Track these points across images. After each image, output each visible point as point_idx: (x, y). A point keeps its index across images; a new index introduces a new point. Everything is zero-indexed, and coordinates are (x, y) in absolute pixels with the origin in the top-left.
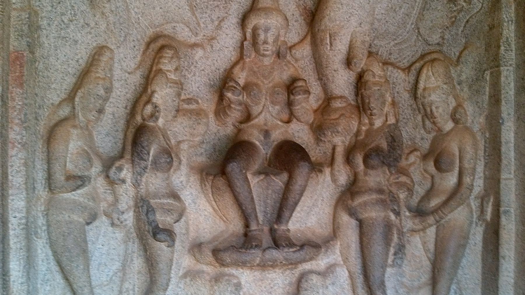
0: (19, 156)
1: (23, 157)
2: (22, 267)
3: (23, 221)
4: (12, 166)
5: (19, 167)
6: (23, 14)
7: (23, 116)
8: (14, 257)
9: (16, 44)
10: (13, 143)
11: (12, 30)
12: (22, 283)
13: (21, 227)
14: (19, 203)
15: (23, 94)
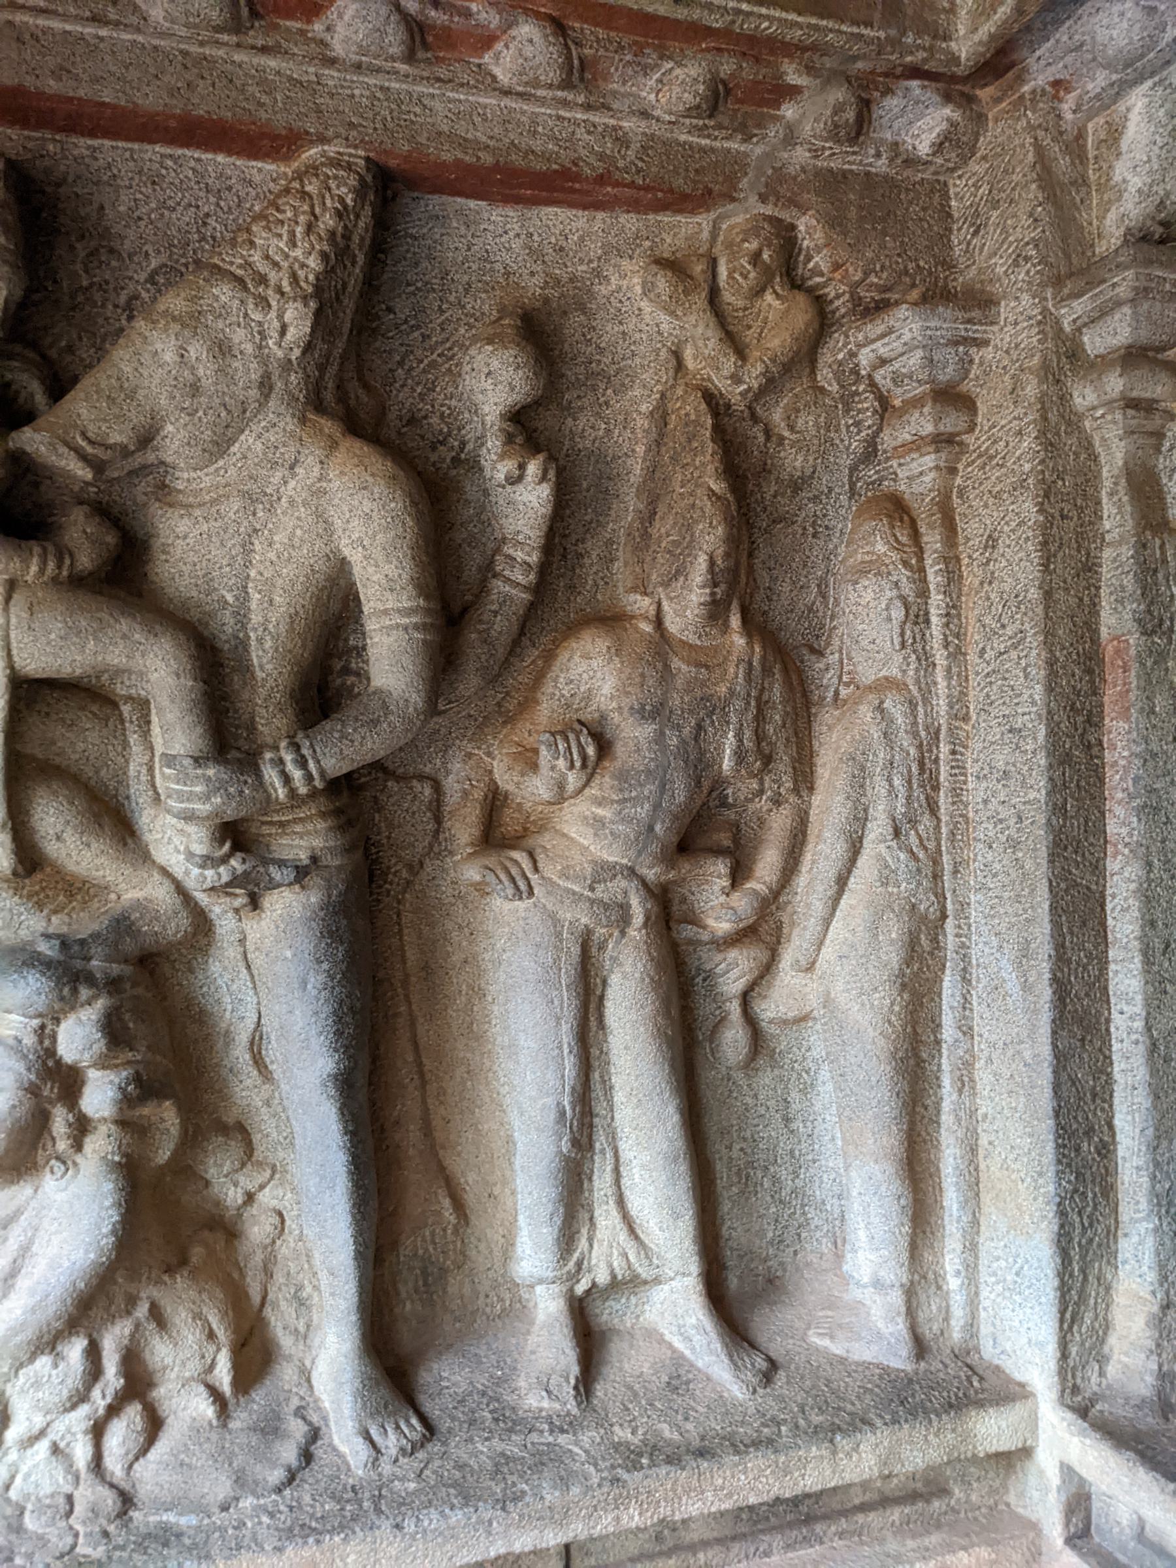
0: (1126, 874)
1: (1133, 877)
2: (1137, 1131)
3: (1139, 1024)
4: (1114, 896)
5: (1126, 899)
6: (1124, 549)
7: (1130, 782)
8: (1122, 1103)
9: (1113, 621)
10: (1115, 846)
11: (1103, 592)
12: (1138, 1168)
13: (1134, 1037)
14: (1127, 982)
15: (1129, 732)
